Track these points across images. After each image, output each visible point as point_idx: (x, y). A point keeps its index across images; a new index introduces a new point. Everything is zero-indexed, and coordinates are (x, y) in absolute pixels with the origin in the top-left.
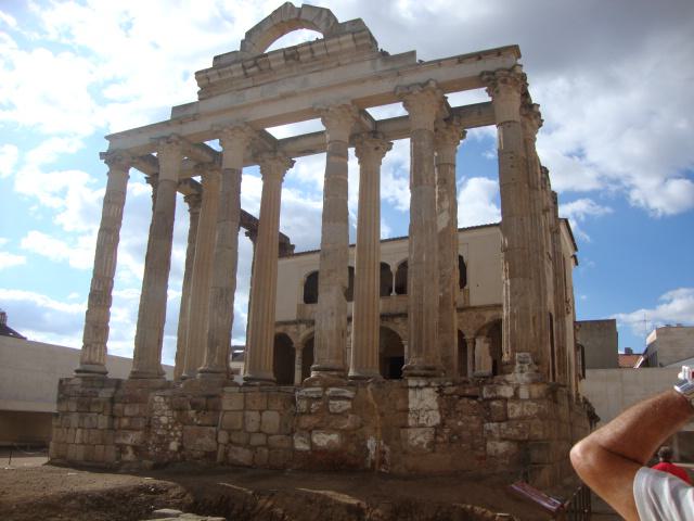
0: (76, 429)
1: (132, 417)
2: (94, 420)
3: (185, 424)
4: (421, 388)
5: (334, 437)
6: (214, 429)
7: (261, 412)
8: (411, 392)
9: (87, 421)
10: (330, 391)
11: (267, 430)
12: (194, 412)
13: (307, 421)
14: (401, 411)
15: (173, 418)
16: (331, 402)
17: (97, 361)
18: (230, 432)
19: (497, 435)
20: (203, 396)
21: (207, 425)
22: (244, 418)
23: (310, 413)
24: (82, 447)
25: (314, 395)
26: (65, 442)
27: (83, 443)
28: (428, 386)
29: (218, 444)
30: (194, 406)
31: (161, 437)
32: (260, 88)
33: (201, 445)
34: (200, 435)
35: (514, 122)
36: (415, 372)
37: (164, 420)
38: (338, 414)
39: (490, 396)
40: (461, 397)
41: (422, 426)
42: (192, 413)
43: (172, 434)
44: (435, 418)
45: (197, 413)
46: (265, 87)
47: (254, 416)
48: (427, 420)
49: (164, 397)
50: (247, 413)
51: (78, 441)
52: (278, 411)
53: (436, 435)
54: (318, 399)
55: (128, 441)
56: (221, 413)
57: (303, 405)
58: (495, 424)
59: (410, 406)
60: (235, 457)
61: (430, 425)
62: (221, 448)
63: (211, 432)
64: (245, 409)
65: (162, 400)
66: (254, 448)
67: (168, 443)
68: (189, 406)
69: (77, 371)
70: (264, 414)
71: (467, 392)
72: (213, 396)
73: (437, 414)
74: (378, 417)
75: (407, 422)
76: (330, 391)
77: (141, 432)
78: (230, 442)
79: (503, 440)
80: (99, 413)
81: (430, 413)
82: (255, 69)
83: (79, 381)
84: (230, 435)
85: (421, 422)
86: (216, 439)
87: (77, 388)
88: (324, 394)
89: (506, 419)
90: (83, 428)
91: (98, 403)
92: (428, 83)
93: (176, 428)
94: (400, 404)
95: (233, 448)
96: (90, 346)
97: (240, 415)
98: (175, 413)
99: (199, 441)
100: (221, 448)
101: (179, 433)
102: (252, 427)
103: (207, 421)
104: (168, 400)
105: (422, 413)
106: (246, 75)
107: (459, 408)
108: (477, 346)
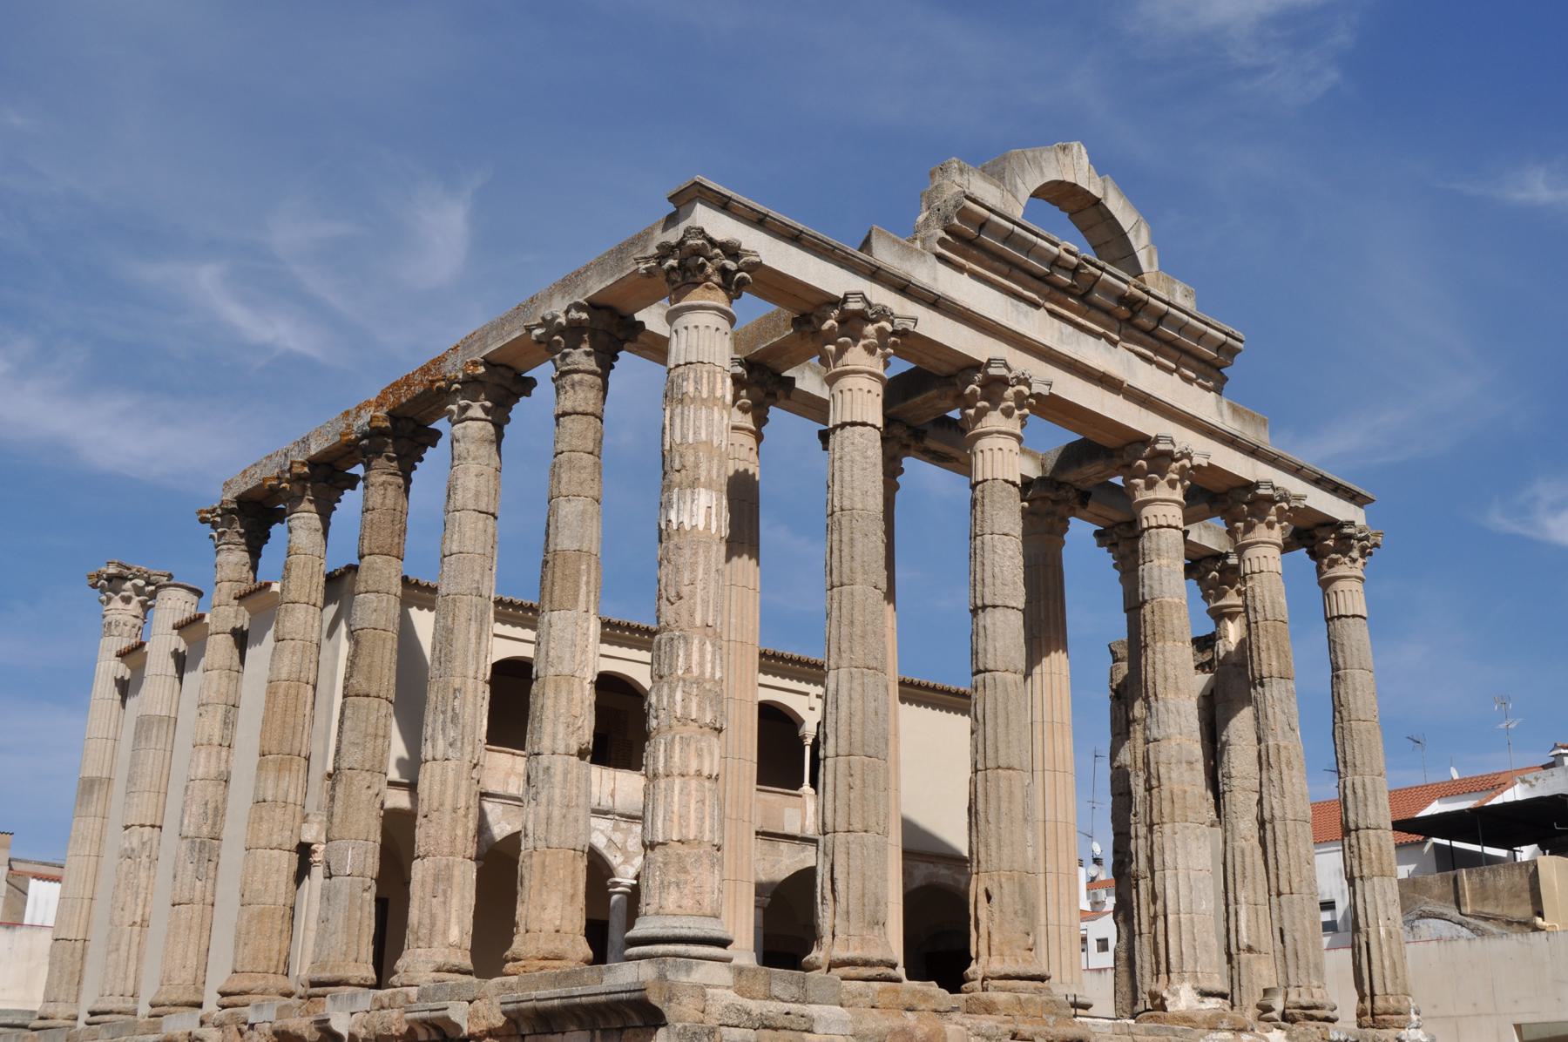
32: (1056, 322)
82: (1066, 280)
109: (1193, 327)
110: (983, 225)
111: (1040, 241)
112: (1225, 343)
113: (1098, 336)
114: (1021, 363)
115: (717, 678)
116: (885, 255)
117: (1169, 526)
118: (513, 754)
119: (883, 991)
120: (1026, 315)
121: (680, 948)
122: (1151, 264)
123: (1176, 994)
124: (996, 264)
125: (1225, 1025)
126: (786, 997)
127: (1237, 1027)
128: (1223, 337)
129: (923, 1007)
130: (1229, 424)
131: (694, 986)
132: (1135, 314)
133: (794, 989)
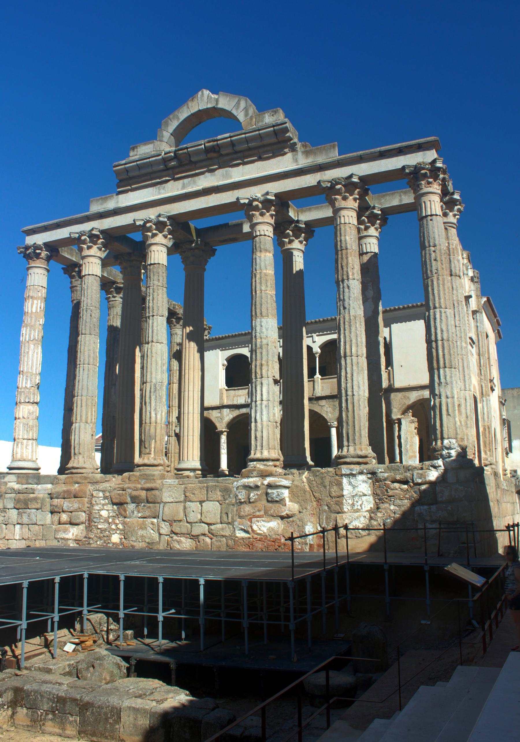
1: (71, 512)
2: (33, 517)
3: (125, 517)
4: (354, 475)
5: (274, 524)
6: (155, 520)
7: (201, 502)
8: (345, 480)
10: (268, 480)
11: (208, 521)
13: (247, 509)
14: (338, 497)
15: (113, 511)
16: (269, 491)
17: (30, 458)
18: (171, 522)
19: (428, 518)
20: (143, 489)
21: (149, 517)
22: (185, 508)
23: (250, 502)
25: (252, 485)
28: (361, 473)
31: (102, 530)
32: (181, 181)
33: (142, 536)
35: (436, 215)
36: (348, 460)
37: (104, 513)
38: (277, 501)
39: (420, 481)
40: (393, 482)
41: (357, 511)
42: (131, 507)
43: (113, 527)
44: (368, 503)
45: (137, 506)
46: (186, 181)
48: (361, 506)
49: (103, 491)
50: (188, 504)
51: (17, 538)
53: (371, 518)
54: (257, 487)
55: (70, 536)
56: (162, 505)
57: (242, 495)
58: (426, 507)
59: (345, 493)
60: (178, 547)
61: (364, 509)
63: (152, 523)
64: (185, 501)
65: (101, 494)
66: (195, 537)
67: (109, 537)
68: (129, 500)
69: (10, 468)
70: (203, 504)
71: (398, 478)
72: (152, 489)
73: (371, 499)
74: (315, 503)
75: (342, 509)
76: (268, 480)
77: (82, 527)
78: (173, 532)
79: (433, 522)
80: (37, 509)
81: (364, 498)
83: (13, 478)
84: (171, 525)
85: (356, 507)
86: (159, 530)
87: (10, 485)
88: (263, 484)
89: (436, 502)
91: (35, 499)
92: (351, 176)
94: (334, 490)
95: (175, 537)
96: (22, 444)
97: (181, 507)
98: (115, 507)
99: (140, 532)
101: (120, 526)
102: (194, 517)
103: (147, 513)
104: (108, 494)
105: (356, 499)
106: (167, 169)
107: (391, 493)
108: (403, 427)
109: (250, 136)
110: (127, 170)
111: (151, 159)
112: (274, 130)
113: (202, 173)
114: (140, 216)
115: (24, 386)
116: (95, 208)
117: (265, 235)
118: (235, 390)
119: (68, 478)
120: (164, 188)
122: (246, 115)
124: (143, 179)
125: (255, 473)
126: (33, 483)
127: (264, 474)
128: (272, 129)
129: (83, 481)
130: (303, 162)
132: (219, 152)
133: (35, 480)
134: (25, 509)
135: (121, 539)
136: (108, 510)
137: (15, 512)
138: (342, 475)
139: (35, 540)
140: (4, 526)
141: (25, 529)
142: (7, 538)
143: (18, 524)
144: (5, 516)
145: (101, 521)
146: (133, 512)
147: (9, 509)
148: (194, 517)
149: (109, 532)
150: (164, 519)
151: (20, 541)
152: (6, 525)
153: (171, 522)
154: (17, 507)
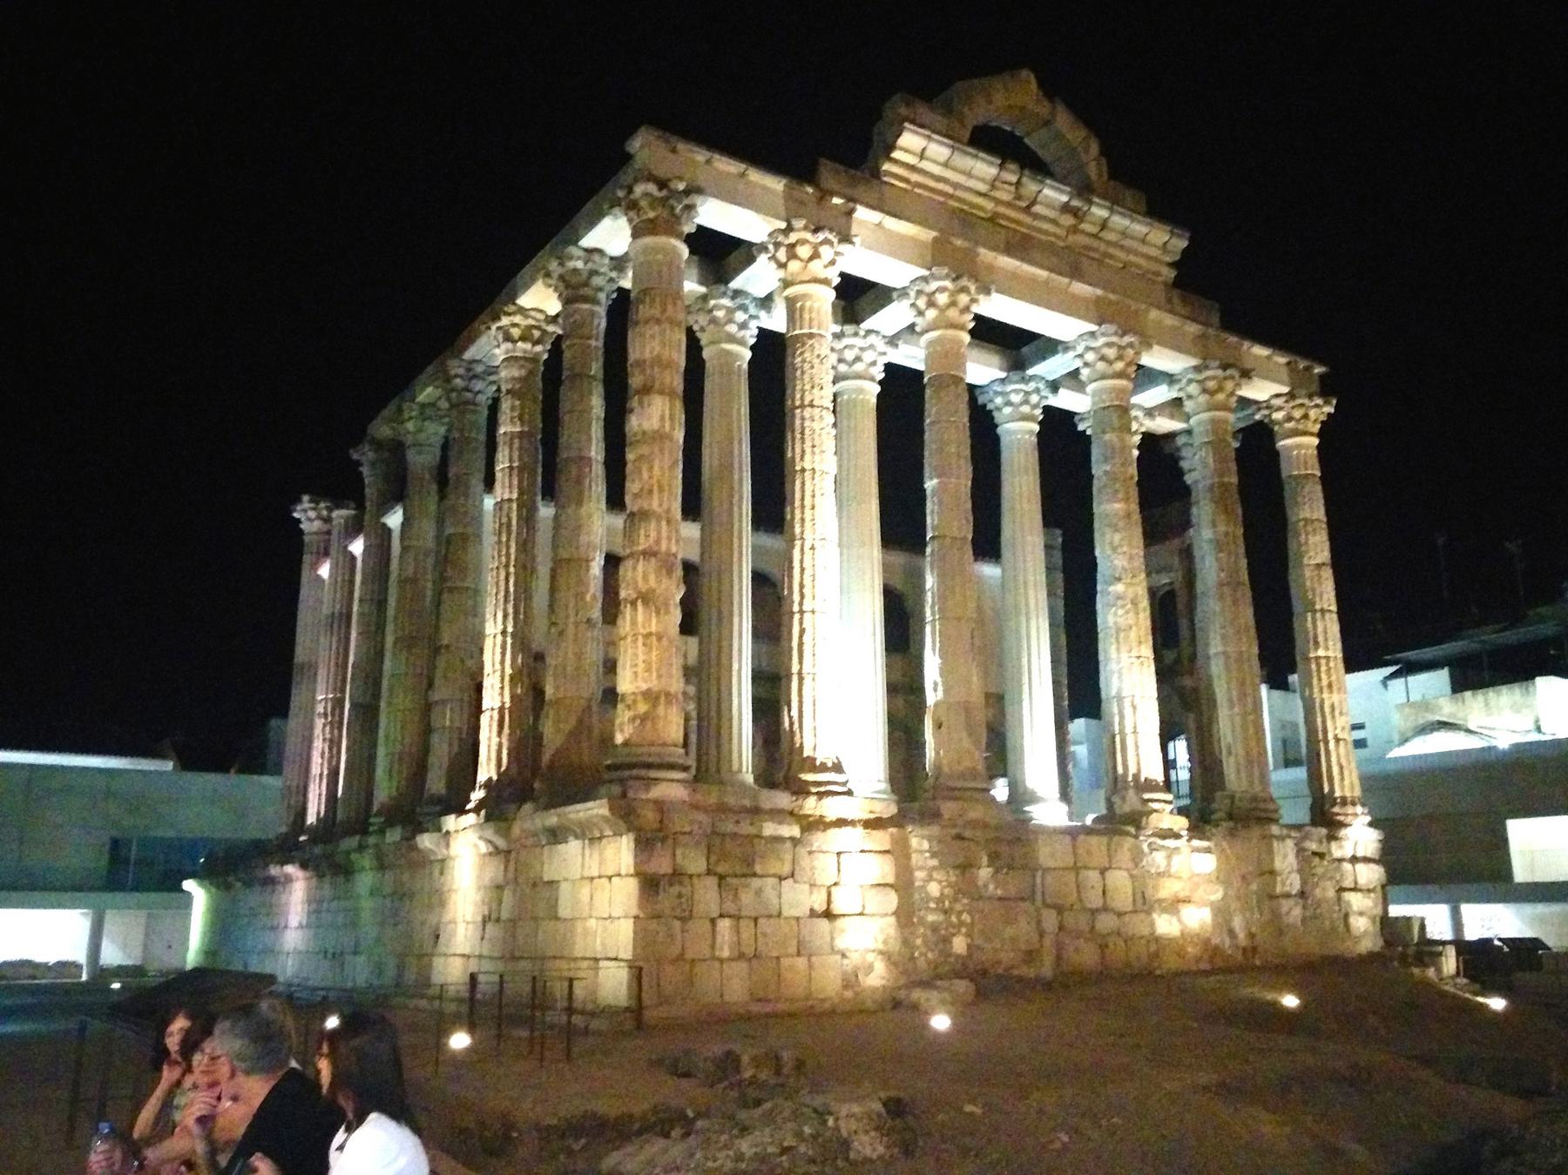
0: (713, 921)
7: (1103, 872)
8: (1275, 844)
9: (746, 898)
12: (990, 870)
18: (1060, 910)
24: (743, 965)
26: (681, 957)
27: (741, 956)
29: (1042, 934)
30: (994, 858)
31: (935, 928)
33: (1013, 939)
34: (1010, 921)
42: (985, 873)
47: (1093, 876)
51: (726, 953)
52: (1127, 870)
56: (1039, 873)
62: (1048, 941)
68: (985, 860)
70: (1108, 874)
80: (781, 879)
90: (737, 918)
93: (958, 907)
99: (1009, 931)
100: (1048, 941)
101: (966, 917)
121: (643, 772)
123: (1123, 799)
131: (648, 801)
134: (744, 875)
135: (969, 947)
136: (940, 882)
137: (712, 882)
138: (1273, 836)
139: (778, 958)
140: (677, 924)
141: (747, 930)
142: (689, 955)
143: (721, 916)
144: (680, 896)
145: (932, 905)
146: (986, 886)
147: (691, 876)
148: (1094, 900)
149: (946, 929)
150: (1049, 901)
151: (733, 964)
152: (683, 920)
153: (1060, 910)
154: (720, 869)
